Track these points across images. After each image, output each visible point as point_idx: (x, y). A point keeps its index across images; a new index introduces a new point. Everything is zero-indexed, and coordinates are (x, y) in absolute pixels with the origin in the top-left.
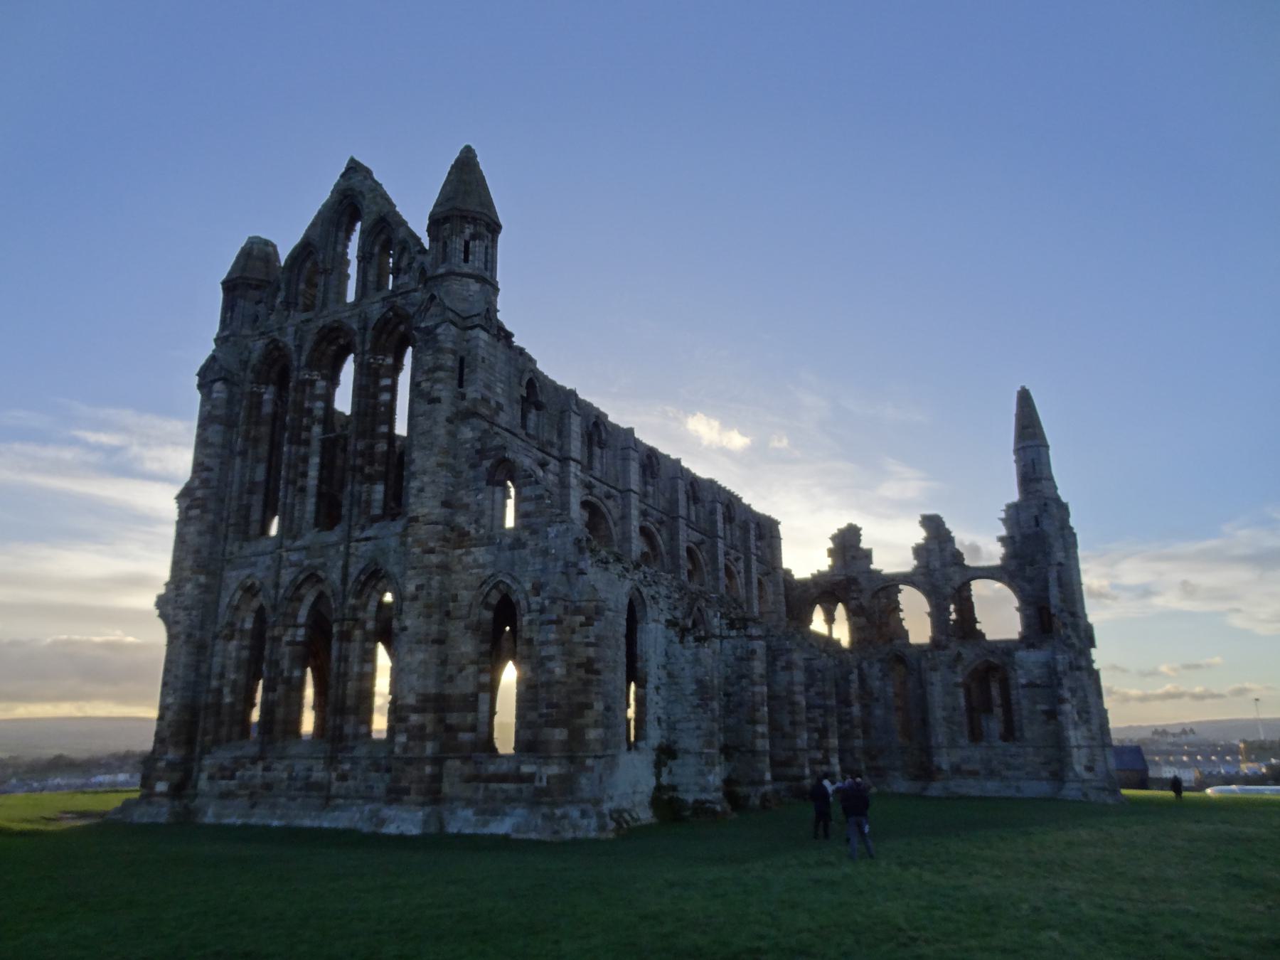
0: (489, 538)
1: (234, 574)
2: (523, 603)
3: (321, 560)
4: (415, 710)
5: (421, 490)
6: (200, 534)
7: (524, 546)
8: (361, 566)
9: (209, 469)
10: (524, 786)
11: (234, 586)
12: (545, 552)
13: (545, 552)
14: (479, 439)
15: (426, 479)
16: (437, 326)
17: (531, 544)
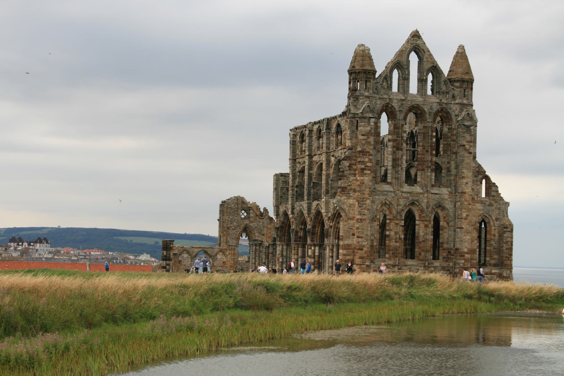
0: (481, 201)
1: (377, 197)
2: (492, 223)
3: (417, 198)
4: (467, 253)
5: (467, 183)
6: (371, 181)
7: (492, 205)
8: (434, 203)
9: (371, 155)
10: (493, 276)
11: (377, 202)
12: (499, 209)
13: (499, 209)
14: (478, 167)
15: (468, 180)
16: (471, 126)
17: (495, 205)
